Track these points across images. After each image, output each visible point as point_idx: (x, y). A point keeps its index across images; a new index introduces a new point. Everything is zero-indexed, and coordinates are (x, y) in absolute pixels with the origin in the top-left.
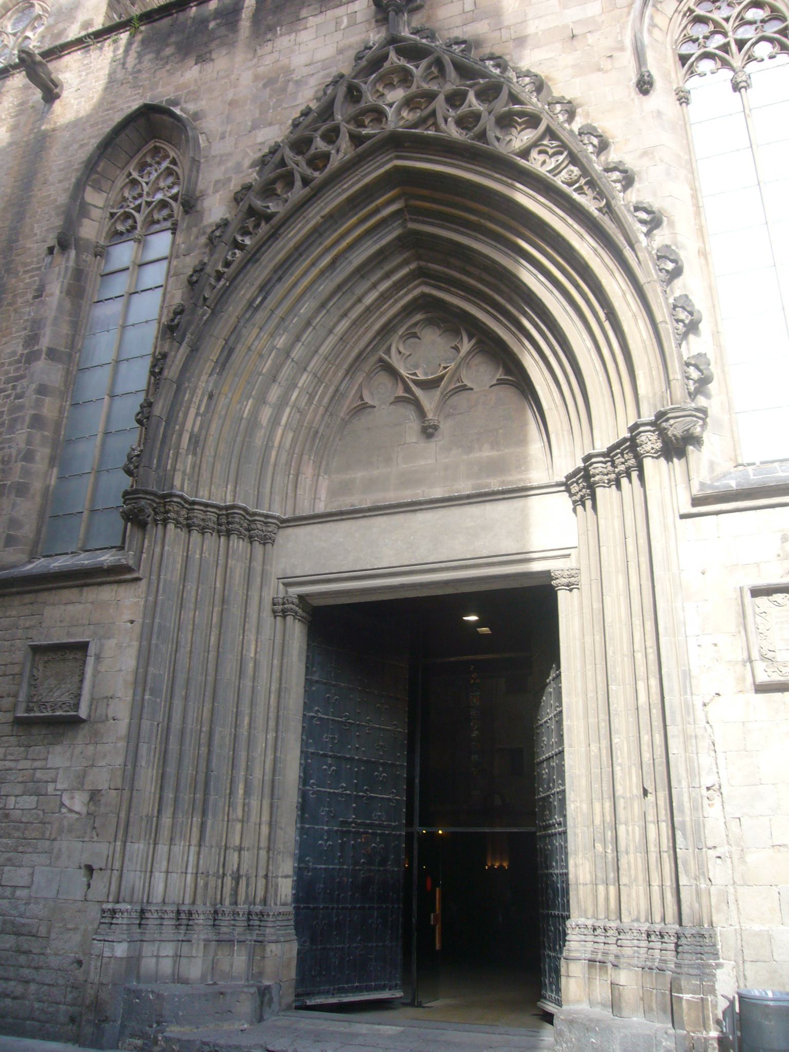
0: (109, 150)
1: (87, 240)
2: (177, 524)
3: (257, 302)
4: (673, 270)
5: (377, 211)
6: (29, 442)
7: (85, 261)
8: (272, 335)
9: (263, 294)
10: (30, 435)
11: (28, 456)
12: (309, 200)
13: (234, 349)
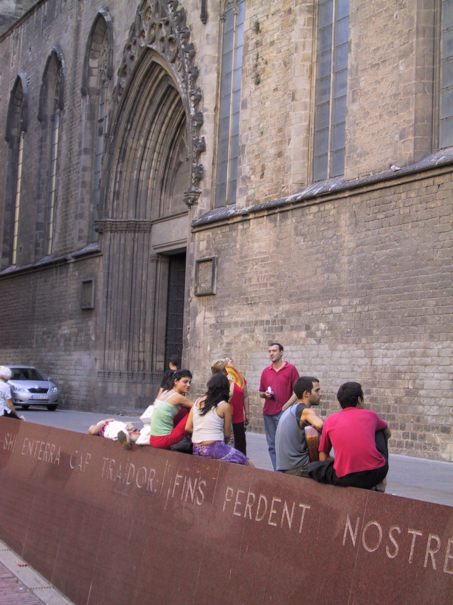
0: (94, 37)
2: (111, 231)
4: (197, 125)
5: (157, 77)
6: (82, 194)
8: (138, 140)
11: (82, 201)
12: (133, 78)
13: (126, 150)
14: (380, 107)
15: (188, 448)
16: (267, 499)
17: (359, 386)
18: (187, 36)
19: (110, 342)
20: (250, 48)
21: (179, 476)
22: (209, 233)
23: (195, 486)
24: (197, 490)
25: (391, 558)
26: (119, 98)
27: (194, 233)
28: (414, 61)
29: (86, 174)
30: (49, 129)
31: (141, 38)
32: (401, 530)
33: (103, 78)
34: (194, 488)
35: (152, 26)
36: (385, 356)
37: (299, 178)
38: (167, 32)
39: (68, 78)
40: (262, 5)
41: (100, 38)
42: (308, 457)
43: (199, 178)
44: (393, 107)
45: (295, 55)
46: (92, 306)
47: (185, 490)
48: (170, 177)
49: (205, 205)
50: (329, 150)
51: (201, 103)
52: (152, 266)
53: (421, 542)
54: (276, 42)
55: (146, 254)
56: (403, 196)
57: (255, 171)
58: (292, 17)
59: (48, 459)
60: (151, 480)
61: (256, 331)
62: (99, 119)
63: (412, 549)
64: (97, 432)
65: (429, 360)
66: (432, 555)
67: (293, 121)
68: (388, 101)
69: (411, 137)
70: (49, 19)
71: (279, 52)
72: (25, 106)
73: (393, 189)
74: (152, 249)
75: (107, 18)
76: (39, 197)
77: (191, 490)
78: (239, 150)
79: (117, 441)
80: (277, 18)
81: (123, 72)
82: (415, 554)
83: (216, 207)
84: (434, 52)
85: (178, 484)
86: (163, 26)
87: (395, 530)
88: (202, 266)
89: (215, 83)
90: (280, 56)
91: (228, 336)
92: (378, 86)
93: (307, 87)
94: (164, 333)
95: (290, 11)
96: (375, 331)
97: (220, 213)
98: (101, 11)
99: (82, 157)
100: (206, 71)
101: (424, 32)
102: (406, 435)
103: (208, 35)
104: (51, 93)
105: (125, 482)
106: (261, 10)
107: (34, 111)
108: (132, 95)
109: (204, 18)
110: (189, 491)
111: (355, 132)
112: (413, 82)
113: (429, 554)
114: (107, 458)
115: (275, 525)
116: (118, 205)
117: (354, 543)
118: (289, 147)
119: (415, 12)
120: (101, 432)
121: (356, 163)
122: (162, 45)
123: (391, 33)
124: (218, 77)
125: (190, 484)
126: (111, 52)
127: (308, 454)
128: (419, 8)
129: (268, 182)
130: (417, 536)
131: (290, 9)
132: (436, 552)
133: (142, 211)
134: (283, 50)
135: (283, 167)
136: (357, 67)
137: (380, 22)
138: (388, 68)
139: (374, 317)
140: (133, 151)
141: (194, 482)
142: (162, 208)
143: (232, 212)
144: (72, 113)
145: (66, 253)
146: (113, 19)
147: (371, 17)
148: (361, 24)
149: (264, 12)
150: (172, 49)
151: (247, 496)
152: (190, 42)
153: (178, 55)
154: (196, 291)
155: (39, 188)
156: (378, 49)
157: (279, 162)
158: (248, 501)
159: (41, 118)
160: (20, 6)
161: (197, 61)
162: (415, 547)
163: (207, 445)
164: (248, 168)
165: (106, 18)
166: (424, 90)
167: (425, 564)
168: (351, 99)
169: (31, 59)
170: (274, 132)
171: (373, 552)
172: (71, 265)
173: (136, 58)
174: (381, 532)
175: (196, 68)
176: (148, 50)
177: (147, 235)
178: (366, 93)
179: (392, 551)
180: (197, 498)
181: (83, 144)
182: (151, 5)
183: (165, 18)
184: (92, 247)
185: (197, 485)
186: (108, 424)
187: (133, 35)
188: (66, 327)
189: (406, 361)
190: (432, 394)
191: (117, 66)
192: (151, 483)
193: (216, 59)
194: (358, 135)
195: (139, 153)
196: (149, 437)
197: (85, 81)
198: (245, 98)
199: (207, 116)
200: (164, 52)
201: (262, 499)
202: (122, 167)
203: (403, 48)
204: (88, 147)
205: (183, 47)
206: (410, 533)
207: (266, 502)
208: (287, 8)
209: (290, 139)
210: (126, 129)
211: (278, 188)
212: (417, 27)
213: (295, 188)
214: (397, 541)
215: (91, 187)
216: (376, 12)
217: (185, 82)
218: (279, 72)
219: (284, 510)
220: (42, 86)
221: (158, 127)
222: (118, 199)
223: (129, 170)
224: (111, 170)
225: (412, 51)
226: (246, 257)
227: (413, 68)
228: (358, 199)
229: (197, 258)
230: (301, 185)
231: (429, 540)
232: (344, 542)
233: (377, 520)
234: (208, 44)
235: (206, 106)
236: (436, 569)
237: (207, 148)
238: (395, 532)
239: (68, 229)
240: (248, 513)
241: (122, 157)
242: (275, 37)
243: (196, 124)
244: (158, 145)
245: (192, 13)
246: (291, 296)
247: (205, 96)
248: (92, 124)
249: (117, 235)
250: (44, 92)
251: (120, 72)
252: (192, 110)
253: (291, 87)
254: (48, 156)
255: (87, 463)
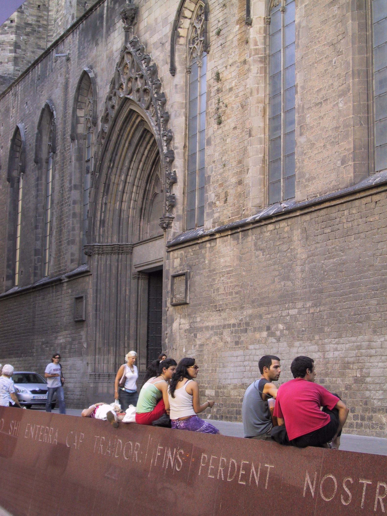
0: (81, 91)
1: (80, 134)
2: (99, 254)
3: (112, 165)
4: (169, 161)
5: (134, 122)
6: (73, 224)
7: (81, 143)
8: (120, 176)
9: (112, 162)
10: (73, 221)
11: (73, 229)
14: (323, 139)
15: (167, 423)
16: (237, 462)
17: (311, 361)
18: (159, 87)
19: (100, 349)
20: (212, 94)
21: (160, 447)
22: (182, 252)
23: (174, 454)
24: (176, 459)
25: (345, 505)
26: (103, 141)
27: (168, 252)
28: (351, 99)
29: (76, 206)
30: (44, 170)
31: (120, 90)
32: (353, 480)
33: (89, 125)
34: (174, 456)
35: (129, 80)
36: (336, 350)
37: (257, 201)
38: (142, 84)
39: (59, 126)
40: (221, 58)
41: (85, 91)
42: (271, 424)
43: (172, 206)
44: (335, 138)
45: (251, 98)
46: (84, 319)
47: (166, 458)
48: (148, 206)
49: (178, 229)
50: (282, 177)
51: (172, 142)
52: (134, 282)
53: (371, 489)
54: (234, 88)
55: (128, 272)
56: (346, 212)
57: (219, 198)
58: (246, 67)
59: (47, 440)
60: (136, 452)
61: (225, 333)
62: (86, 159)
63: (363, 496)
64: (88, 415)
65: (373, 351)
66: (381, 500)
67: (251, 154)
68: (330, 133)
69: (351, 163)
70: (42, 78)
71: (237, 96)
72: (24, 152)
73: (337, 207)
74: (133, 268)
75: (91, 75)
76: (36, 227)
77: (171, 459)
78: (205, 180)
79: (106, 420)
80: (234, 69)
81: (105, 119)
82: (366, 500)
83: (187, 230)
84: (368, 91)
85: (159, 454)
86: (138, 79)
87: (348, 481)
88: (177, 280)
89: (183, 126)
90: (238, 100)
91: (201, 338)
92: (321, 121)
93: (262, 125)
94: (146, 339)
95: (245, 62)
96: (327, 329)
97: (191, 234)
98: (86, 69)
99: (73, 192)
100: (175, 116)
101: (359, 74)
102: (356, 417)
103: (176, 85)
104: (45, 139)
105: (114, 456)
106: (220, 62)
107: (31, 155)
108: (114, 138)
109: (173, 71)
110: (170, 459)
111: (303, 161)
112: (351, 116)
113: (379, 499)
114: (98, 436)
115: (244, 483)
116: (104, 231)
117: (313, 495)
118: (248, 176)
119: (350, 57)
120: (92, 414)
121: (305, 186)
122: (138, 95)
123: (331, 76)
124: (186, 120)
125: (170, 453)
126: (95, 103)
127: (271, 422)
128: (353, 54)
129: (231, 206)
130: (368, 484)
131: (245, 60)
132: (384, 497)
133: (124, 236)
134: (240, 95)
135: (243, 193)
136: (303, 107)
137: (321, 68)
138: (330, 106)
139: (325, 317)
140: (115, 186)
141: (174, 451)
142: (141, 233)
143: (201, 233)
144: (64, 156)
145: (61, 274)
146: (96, 75)
147: (313, 63)
148: (305, 70)
149: (223, 63)
150: (146, 98)
151: (219, 460)
152: (161, 92)
153: (152, 103)
154: (172, 302)
155: (36, 221)
156: (320, 90)
157: (239, 189)
158: (220, 465)
159: (37, 161)
160: (17, 68)
161: (168, 107)
162: (366, 494)
163: (184, 420)
164: (213, 195)
165: (90, 74)
166: (360, 122)
167: (375, 509)
168: (299, 133)
169: (28, 111)
170: (234, 164)
171: (329, 501)
172: (65, 284)
173: (117, 107)
174: (336, 483)
175: (167, 113)
176: (126, 100)
177: (129, 256)
178: (312, 128)
179: (346, 500)
180: (177, 465)
181: (73, 181)
182: (128, 62)
183: (140, 73)
184: (83, 268)
185: (176, 454)
186: (98, 407)
187: (113, 88)
188: (61, 337)
189: (353, 353)
190: (377, 381)
191: (101, 114)
192: (136, 455)
193: (184, 106)
194: (305, 163)
195: (121, 187)
196: (134, 415)
197: (74, 128)
198: (209, 136)
199: (178, 153)
200: (139, 101)
201: (233, 462)
202: (106, 199)
203: (341, 88)
204: (78, 184)
205: (155, 96)
206: (361, 483)
207: (236, 464)
208: (242, 59)
209: (248, 170)
210: (109, 167)
211: (239, 210)
212: (353, 70)
213: (254, 210)
214: (350, 490)
215: (81, 216)
216: (318, 59)
217: (158, 125)
218: (237, 113)
219: (252, 470)
220: (37, 134)
221: (136, 165)
222: (104, 226)
223: (112, 202)
224: (97, 202)
225: (349, 91)
226: (214, 270)
227: (351, 104)
228: (307, 217)
229: (172, 273)
230: (259, 208)
231: (377, 487)
232: (304, 494)
233: (332, 473)
234: (177, 92)
235: (176, 145)
236: (384, 512)
237: (178, 180)
238: (348, 483)
239: (62, 254)
240: (220, 475)
241: (107, 190)
242: (233, 84)
243: (168, 160)
244: (136, 180)
245: (163, 68)
246: (253, 302)
247: (175, 136)
248: (81, 165)
249: (104, 257)
250: (39, 139)
251: (103, 120)
252: (165, 148)
253: (248, 126)
254: (44, 192)
255: (81, 441)
